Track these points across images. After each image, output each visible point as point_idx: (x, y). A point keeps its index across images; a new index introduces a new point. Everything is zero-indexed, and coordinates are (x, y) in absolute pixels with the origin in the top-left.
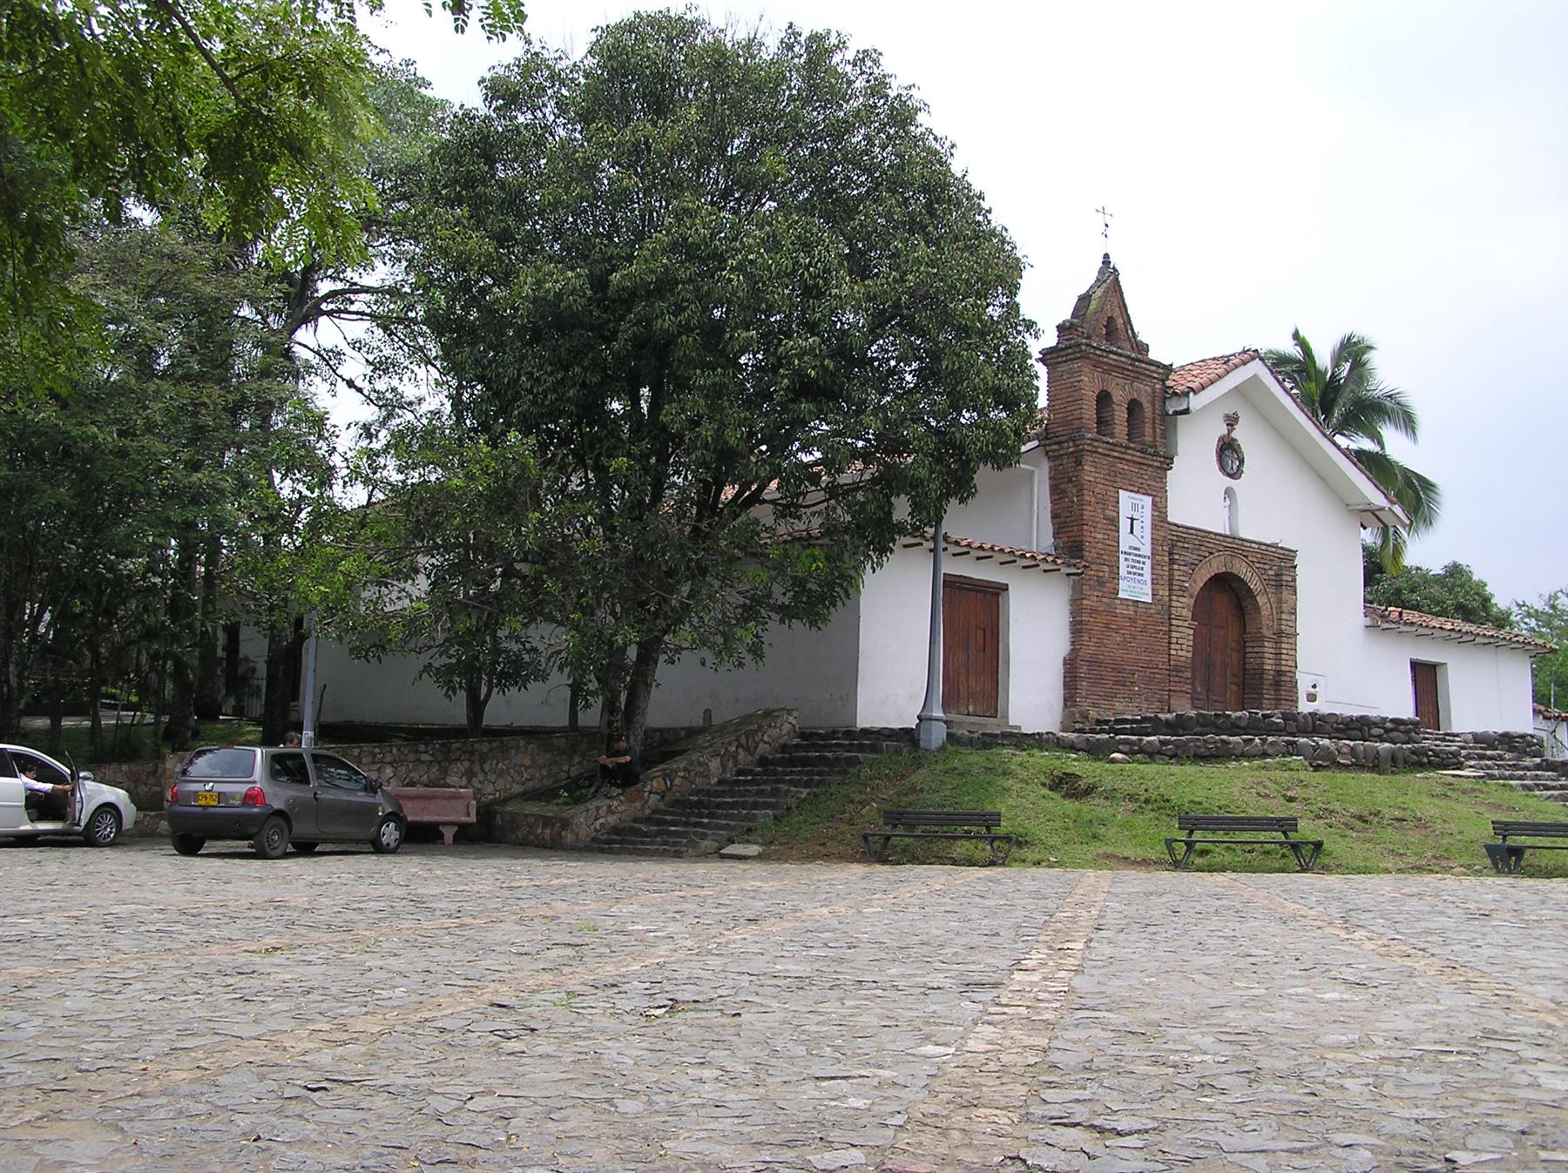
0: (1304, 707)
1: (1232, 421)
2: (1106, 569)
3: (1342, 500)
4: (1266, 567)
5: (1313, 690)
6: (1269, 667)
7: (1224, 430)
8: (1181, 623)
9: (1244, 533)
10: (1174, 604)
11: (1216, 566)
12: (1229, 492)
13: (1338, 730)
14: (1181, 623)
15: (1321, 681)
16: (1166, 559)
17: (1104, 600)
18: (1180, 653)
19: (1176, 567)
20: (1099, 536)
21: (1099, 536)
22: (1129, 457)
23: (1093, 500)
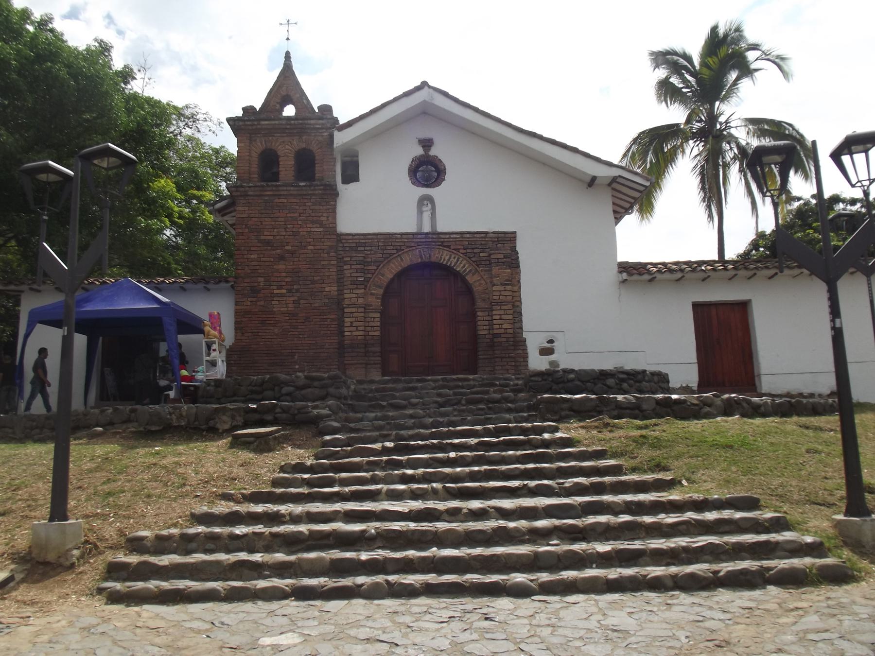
0: (537, 363)
1: (427, 144)
2: (261, 279)
3: (581, 180)
4: (475, 251)
5: (549, 345)
6: (486, 332)
7: (419, 151)
8: (354, 310)
9: (441, 228)
10: (346, 296)
11: (409, 259)
12: (430, 199)
13: (252, 392)
14: (354, 310)
15: (558, 337)
16: (334, 262)
17: (259, 303)
18: (355, 334)
19: (346, 267)
20: (252, 256)
21: (252, 256)
22: (285, 193)
23: (247, 230)
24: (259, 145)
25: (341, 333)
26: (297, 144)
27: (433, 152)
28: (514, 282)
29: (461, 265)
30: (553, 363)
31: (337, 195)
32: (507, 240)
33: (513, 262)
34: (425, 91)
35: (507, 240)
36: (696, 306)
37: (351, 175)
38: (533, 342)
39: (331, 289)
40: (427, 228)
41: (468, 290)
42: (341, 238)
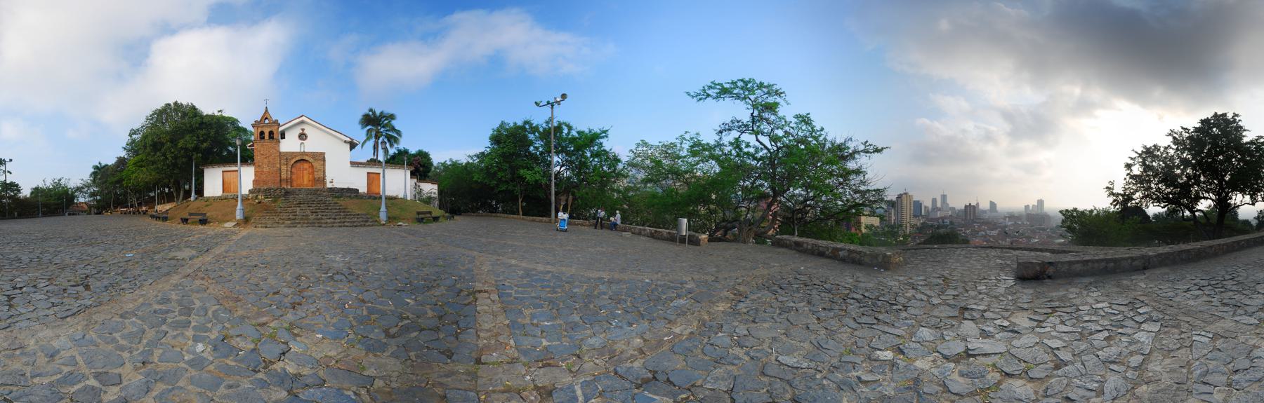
1: (303, 130)
9: (306, 151)
11: (297, 159)
24: (260, 130)
25: (281, 176)
26: (269, 130)
27: (305, 132)
28: (324, 165)
29: (311, 160)
30: (333, 185)
31: (279, 142)
32: (323, 154)
33: (324, 160)
34: (304, 118)
35: (323, 154)
36: (368, 173)
37: (283, 137)
38: (328, 179)
39: (278, 166)
40: (302, 151)
41: (312, 166)
42: (280, 153)
